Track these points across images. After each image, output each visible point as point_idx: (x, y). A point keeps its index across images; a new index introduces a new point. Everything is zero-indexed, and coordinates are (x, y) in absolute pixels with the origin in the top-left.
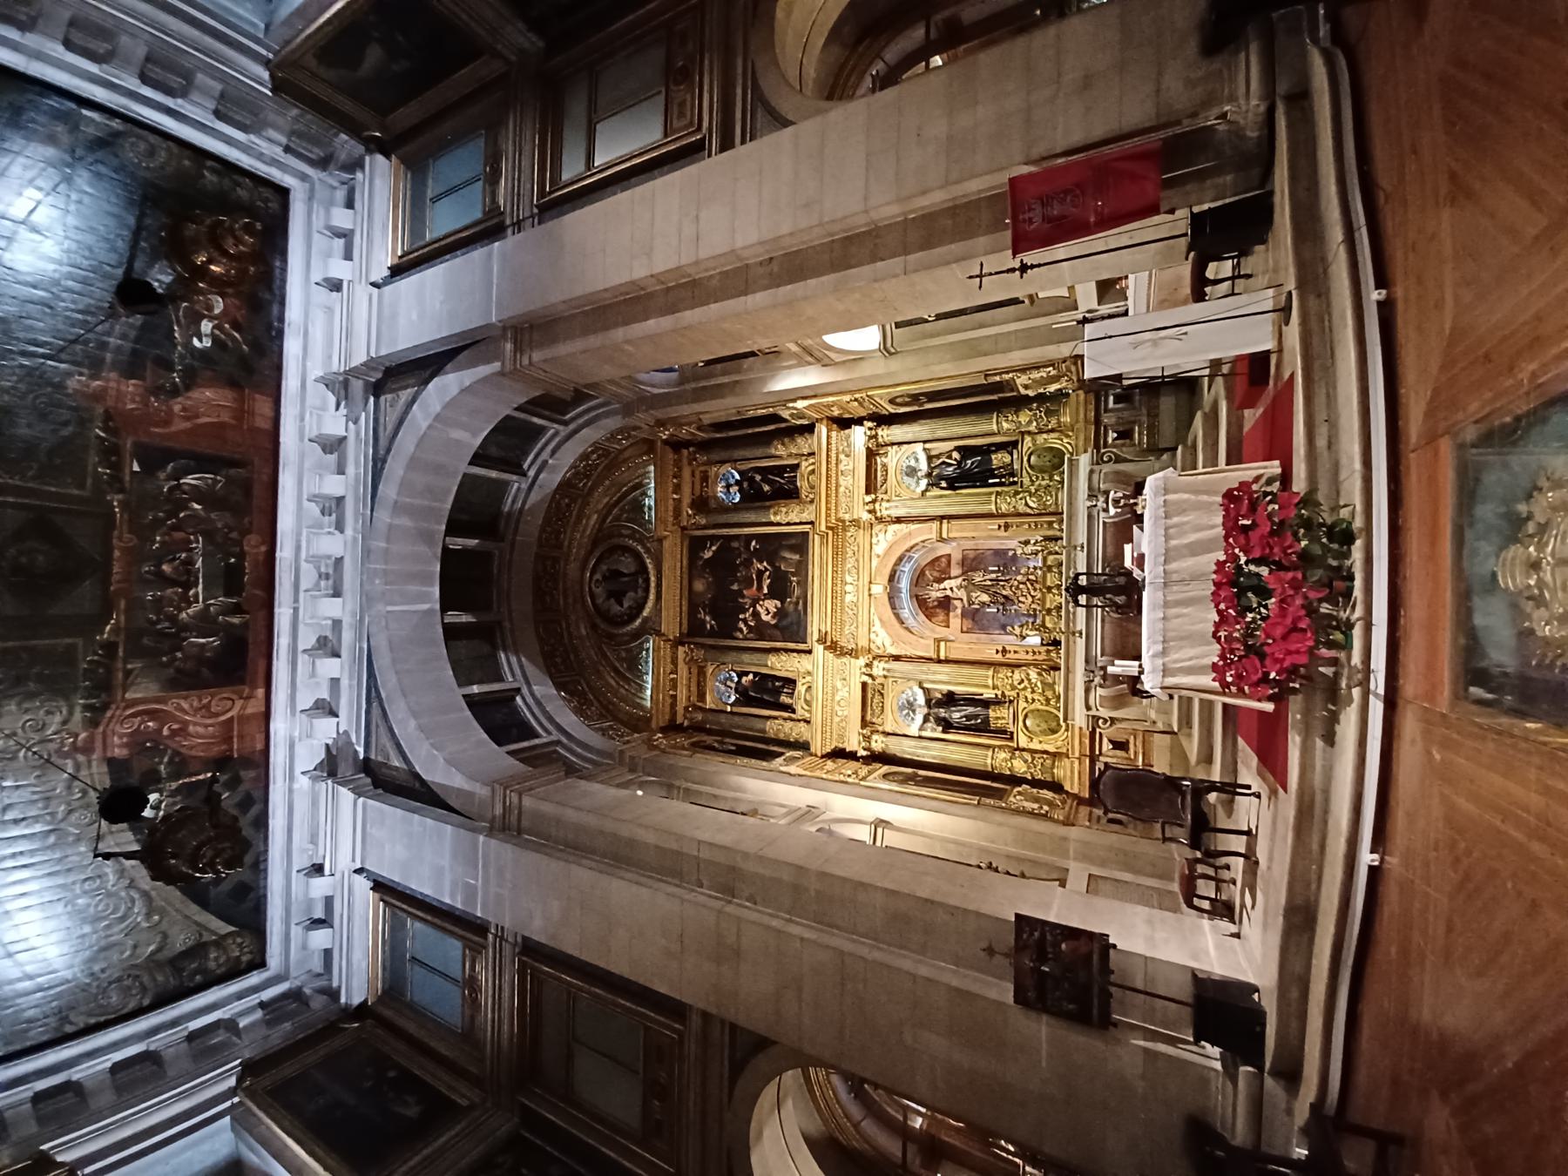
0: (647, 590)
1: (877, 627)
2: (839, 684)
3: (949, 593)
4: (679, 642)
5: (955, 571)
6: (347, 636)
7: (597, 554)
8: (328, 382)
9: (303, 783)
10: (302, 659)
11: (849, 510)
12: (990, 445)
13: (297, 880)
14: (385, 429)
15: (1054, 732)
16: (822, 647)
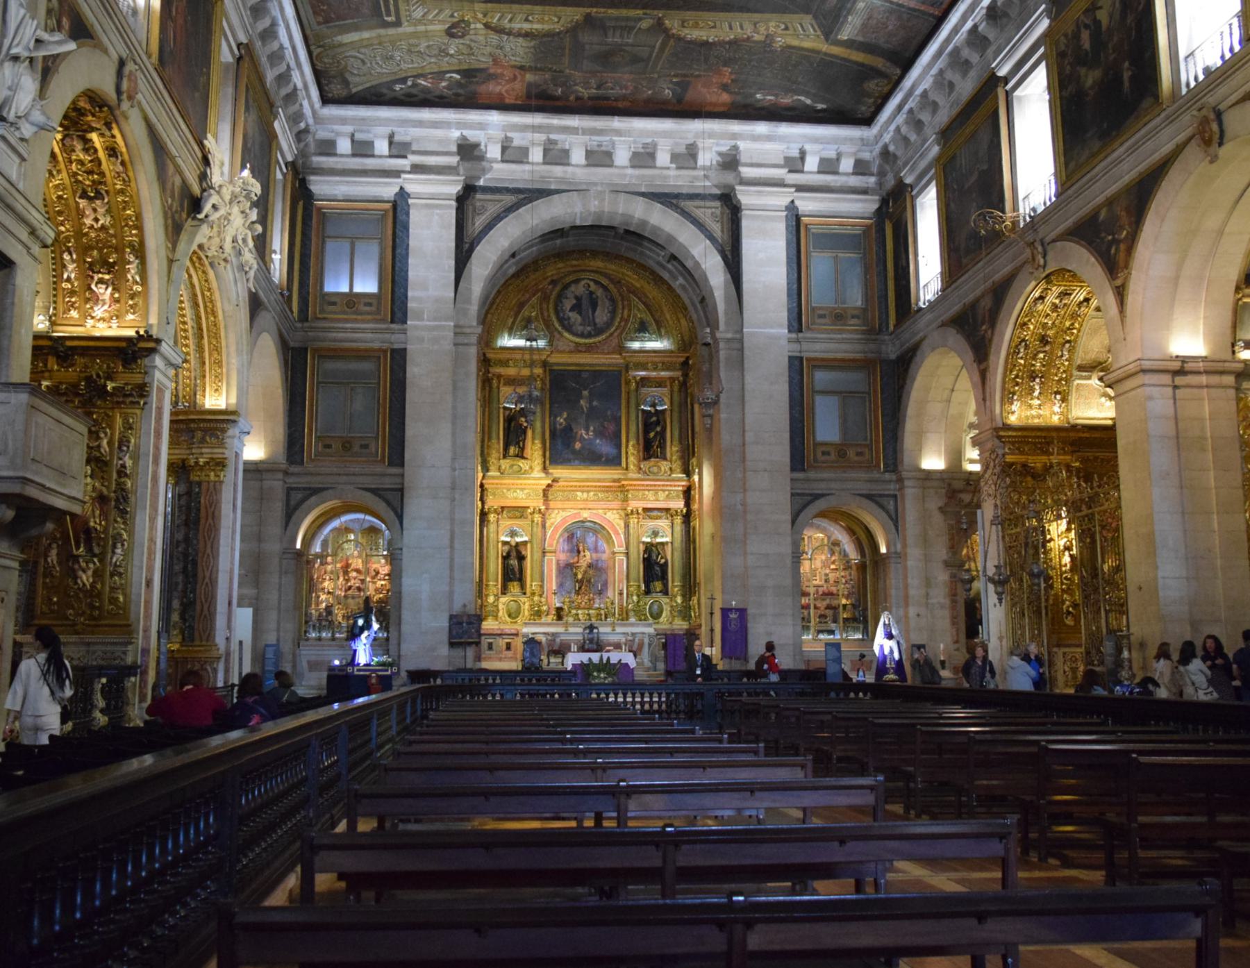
0: (582, 335)
1: (564, 514)
2: (526, 492)
3: (582, 554)
4: (545, 364)
5: (594, 556)
6: (558, 170)
7: (611, 287)
8: (735, 148)
9: (456, 134)
10: (542, 137)
11: (636, 498)
12: (667, 580)
13: (387, 130)
14: (697, 207)
15: (510, 616)
16: (550, 482)
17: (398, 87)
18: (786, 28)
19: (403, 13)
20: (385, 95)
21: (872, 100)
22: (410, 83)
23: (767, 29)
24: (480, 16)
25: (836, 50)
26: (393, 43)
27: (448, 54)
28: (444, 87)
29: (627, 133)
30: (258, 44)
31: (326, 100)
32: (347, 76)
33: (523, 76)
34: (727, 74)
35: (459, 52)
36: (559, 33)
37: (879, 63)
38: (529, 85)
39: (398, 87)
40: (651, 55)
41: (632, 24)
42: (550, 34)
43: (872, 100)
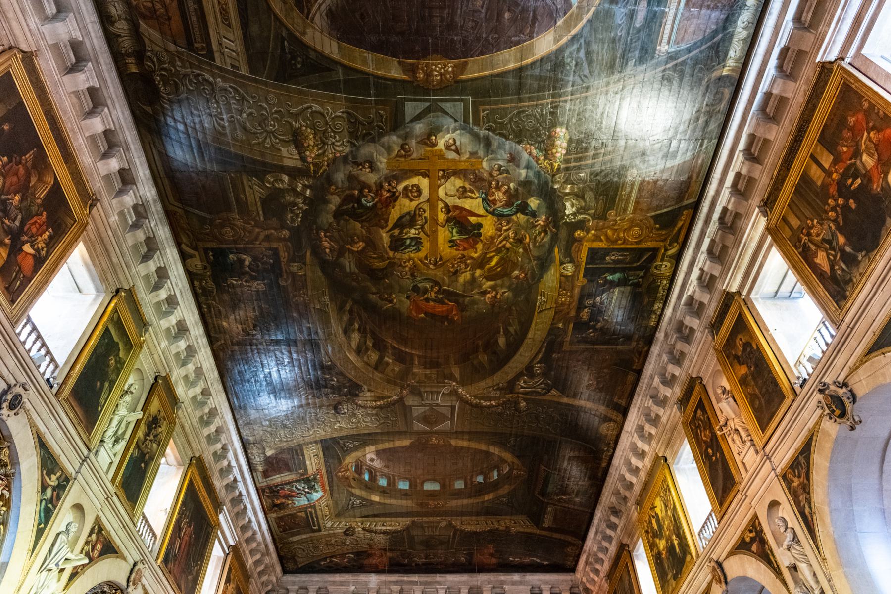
9: (353, 588)
17: (322, 563)
18: (515, 523)
19: (321, 525)
20: (315, 567)
21: (571, 559)
22: (328, 561)
23: (506, 523)
24: (360, 524)
25: (544, 533)
26: (318, 540)
27: (346, 544)
28: (346, 562)
29: (444, 583)
30: (244, 545)
31: (285, 571)
32: (296, 558)
33: (386, 554)
34: (491, 548)
35: (352, 543)
36: (401, 531)
37: (569, 538)
38: (391, 559)
39: (322, 563)
40: (449, 541)
41: (435, 524)
42: (395, 532)
43: (571, 559)
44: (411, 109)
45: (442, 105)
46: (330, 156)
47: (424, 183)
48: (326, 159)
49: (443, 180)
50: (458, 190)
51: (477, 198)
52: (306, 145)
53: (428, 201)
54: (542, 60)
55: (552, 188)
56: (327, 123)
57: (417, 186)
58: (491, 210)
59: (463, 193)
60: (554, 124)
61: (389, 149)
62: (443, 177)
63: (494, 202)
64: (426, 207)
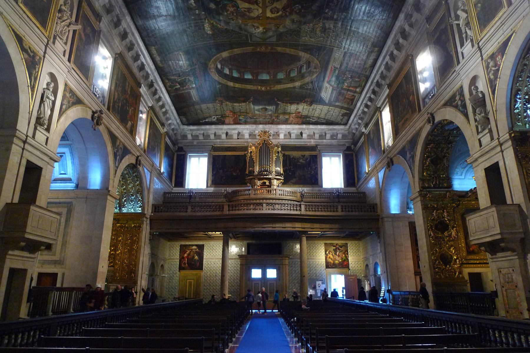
44: (274, 39)
45: (260, 40)
46: (311, 25)
47: (269, 14)
48: (314, 24)
49: (260, 15)
50: (252, 12)
51: (242, 8)
52: (321, 28)
53: (267, 7)
54: (224, 51)
55: (205, 12)
56: (309, 35)
57: (272, 12)
58: (234, 3)
59: (249, 10)
60: (213, 35)
61: (284, 27)
62: (260, 17)
63: (233, 7)
64: (268, 4)
